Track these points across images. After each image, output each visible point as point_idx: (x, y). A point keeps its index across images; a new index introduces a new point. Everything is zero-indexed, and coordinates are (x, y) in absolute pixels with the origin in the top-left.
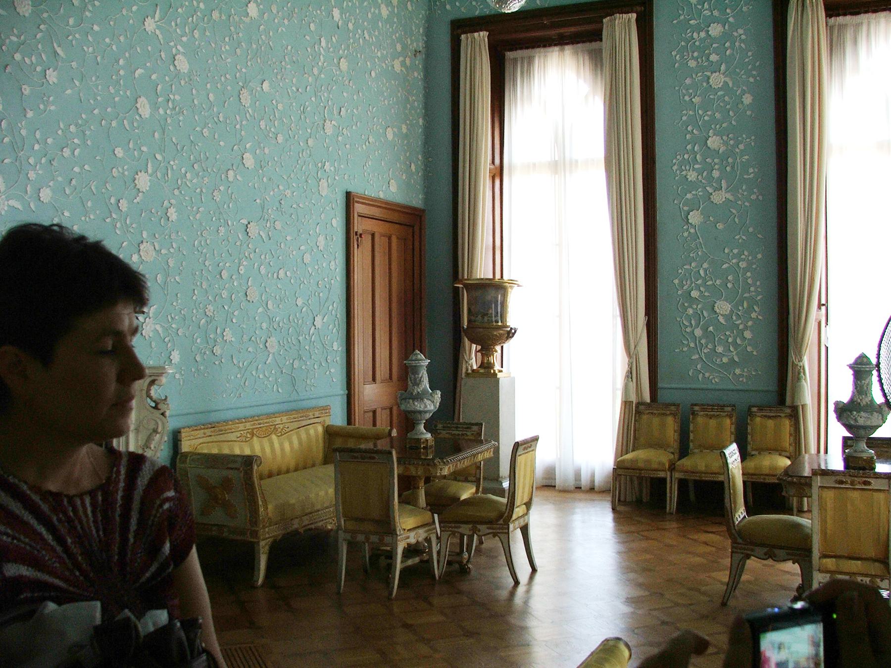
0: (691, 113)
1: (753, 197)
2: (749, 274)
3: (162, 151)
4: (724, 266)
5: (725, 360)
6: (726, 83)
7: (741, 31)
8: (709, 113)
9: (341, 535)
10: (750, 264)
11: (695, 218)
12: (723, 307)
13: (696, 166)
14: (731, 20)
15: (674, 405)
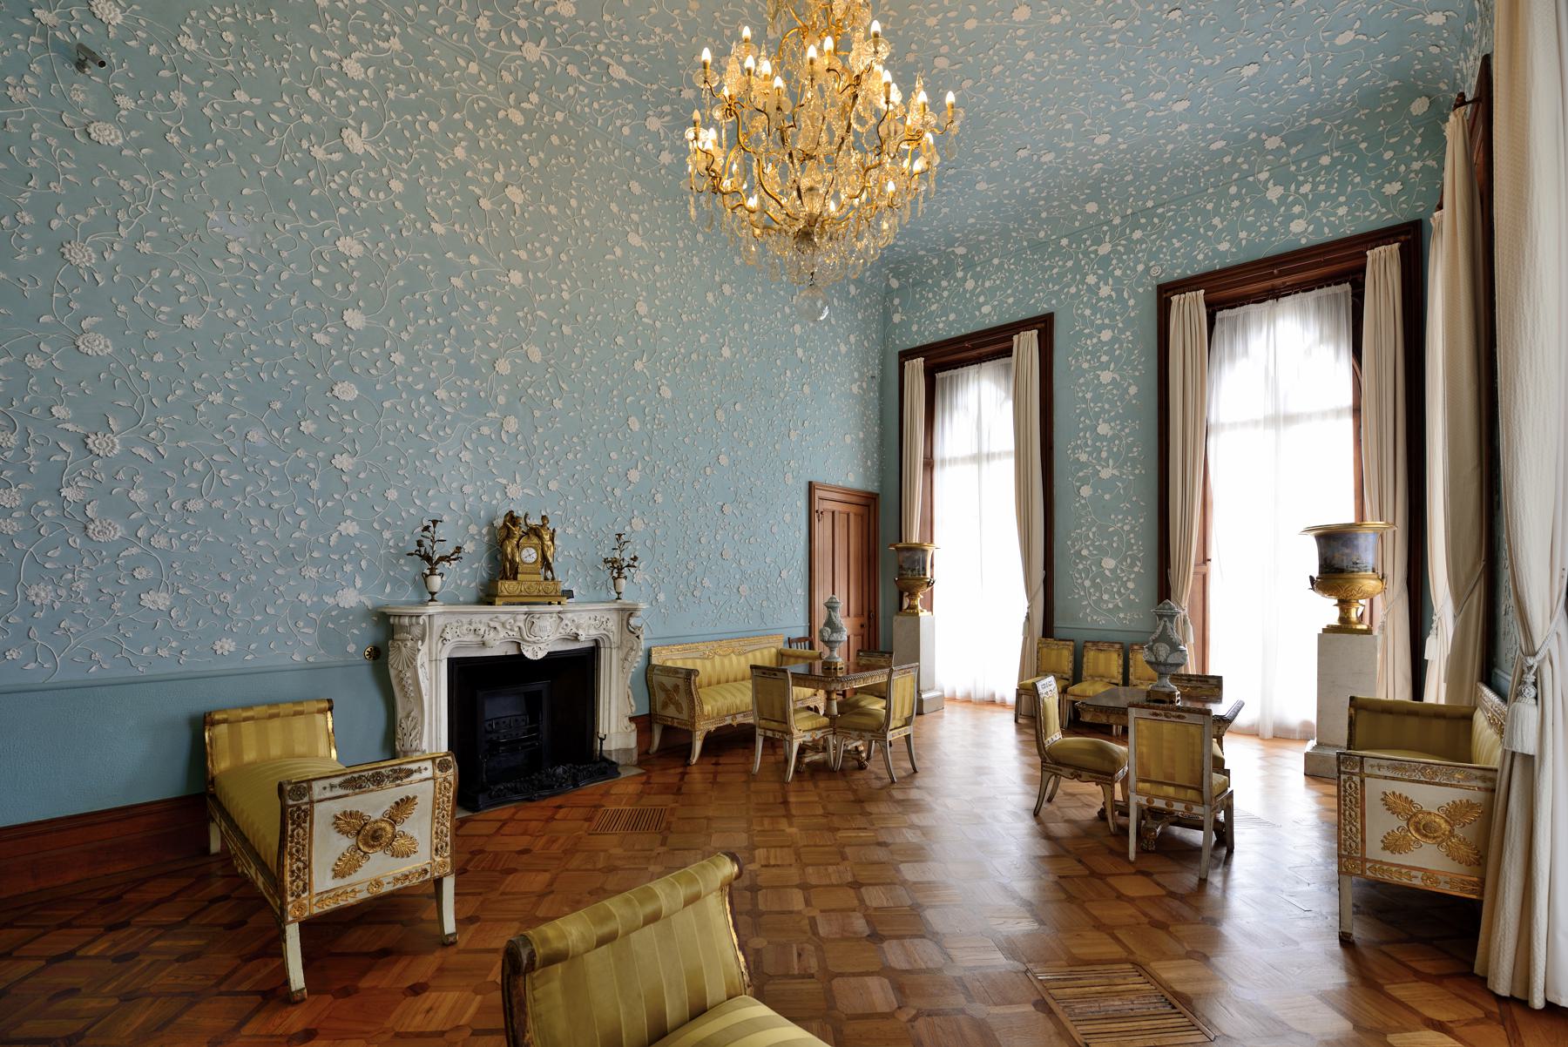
3: (649, 454)
9: (759, 731)
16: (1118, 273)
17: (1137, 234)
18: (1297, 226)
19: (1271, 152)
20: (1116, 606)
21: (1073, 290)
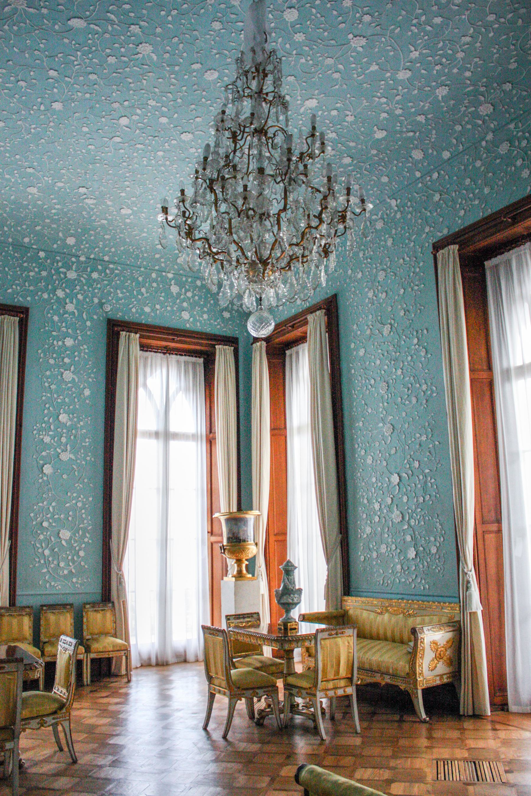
0: (49, 395)
1: (88, 458)
2: (83, 511)
4: (68, 505)
5: (66, 572)
6: (73, 379)
7: (85, 347)
8: (61, 397)
10: (84, 504)
11: (48, 469)
12: (66, 534)
13: (51, 433)
14: (80, 338)
15: (29, 607)
16: (80, 297)
17: (95, 275)
18: (186, 315)
19: (177, 264)
20: (71, 571)
21: (46, 296)
